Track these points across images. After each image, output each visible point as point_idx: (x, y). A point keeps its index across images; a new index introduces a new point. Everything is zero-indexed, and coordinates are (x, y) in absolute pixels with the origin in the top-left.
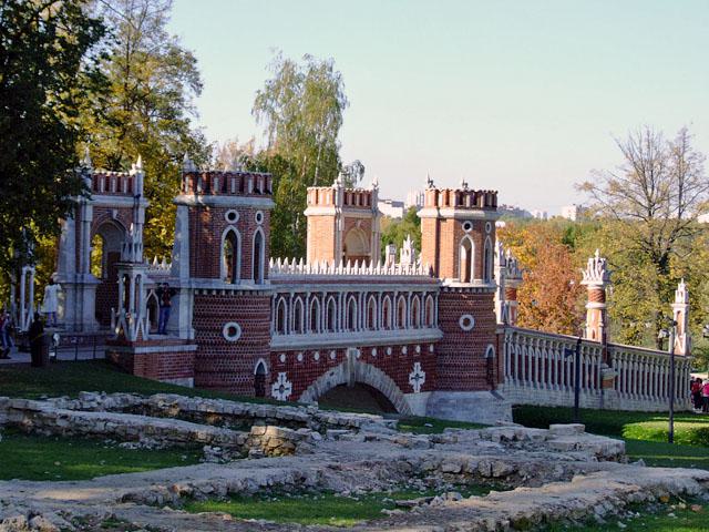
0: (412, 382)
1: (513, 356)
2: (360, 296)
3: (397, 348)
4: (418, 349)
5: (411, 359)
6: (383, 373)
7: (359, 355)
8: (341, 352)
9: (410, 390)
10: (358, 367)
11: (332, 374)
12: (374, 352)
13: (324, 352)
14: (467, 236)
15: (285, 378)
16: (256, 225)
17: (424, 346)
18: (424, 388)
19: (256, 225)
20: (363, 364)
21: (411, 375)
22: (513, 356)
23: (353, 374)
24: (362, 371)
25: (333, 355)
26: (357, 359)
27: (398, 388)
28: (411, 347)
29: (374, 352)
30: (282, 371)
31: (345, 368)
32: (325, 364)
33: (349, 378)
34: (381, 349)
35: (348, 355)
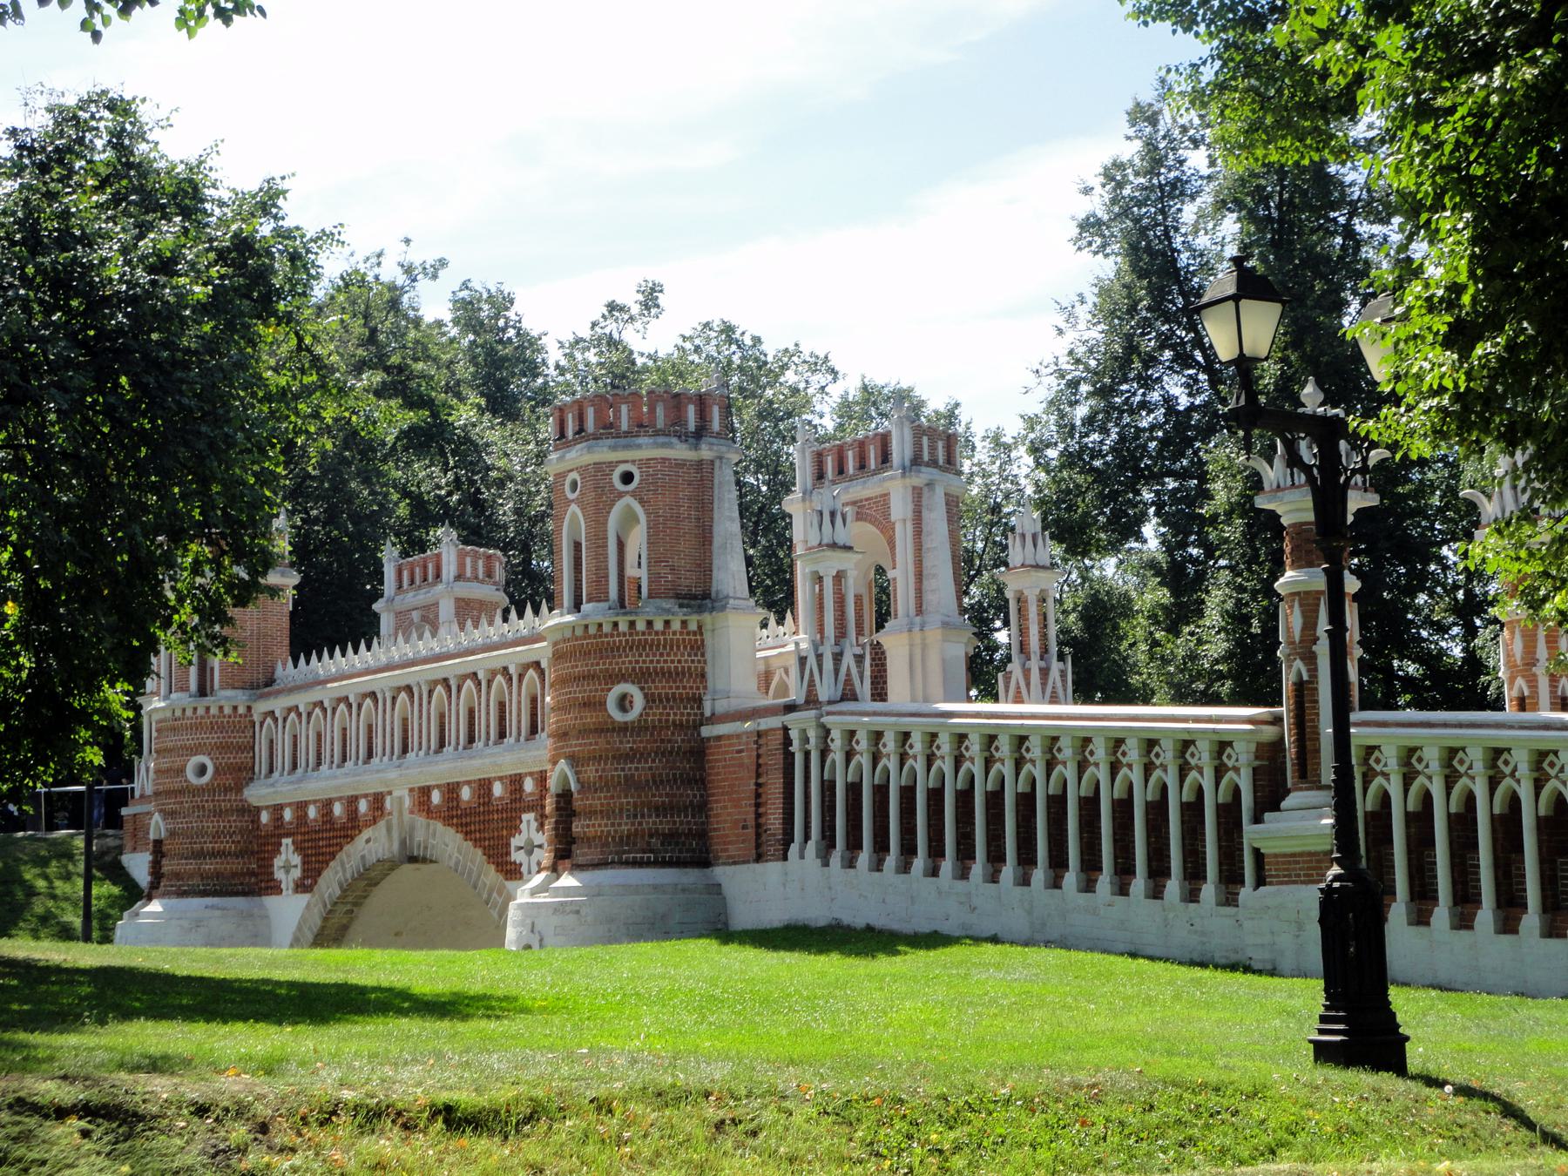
0: (518, 857)
1: (828, 788)
3: (484, 786)
5: (516, 804)
6: (460, 836)
8: (378, 801)
10: (412, 828)
11: (368, 841)
12: (436, 797)
13: (352, 801)
15: (291, 848)
20: (420, 820)
21: (516, 841)
22: (828, 788)
23: (403, 843)
24: (419, 836)
25: (363, 806)
27: (493, 867)
28: (515, 782)
29: (436, 797)
30: (287, 835)
31: (389, 830)
32: (352, 826)
33: (396, 846)
34: (452, 790)
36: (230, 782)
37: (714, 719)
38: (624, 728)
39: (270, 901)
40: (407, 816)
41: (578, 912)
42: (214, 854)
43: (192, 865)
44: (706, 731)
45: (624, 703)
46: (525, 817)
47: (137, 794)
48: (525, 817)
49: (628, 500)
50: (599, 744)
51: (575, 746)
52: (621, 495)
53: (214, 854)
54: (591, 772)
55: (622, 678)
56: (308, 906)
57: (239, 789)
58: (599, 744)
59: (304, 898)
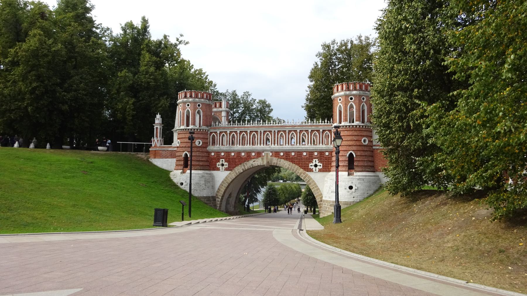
2: (273, 132)
4: (316, 154)
7: (271, 154)
9: (311, 170)
10: (272, 160)
11: (255, 161)
12: (282, 154)
13: (248, 153)
14: (340, 104)
16: (187, 108)
17: (321, 153)
18: (320, 170)
19: (187, 108)
25: (253, 154)
26: (271, 156)
29: (282, 154)
31: (262, 159)
32: (249, 156)
35: (263, 154)
36: (205, 146)
37: (375, 146)
38: (365, 146)
39: (215, 173)
40: (269, 157)
41: (363, 180)
42: (202, 161)
43: (197, 163)
44: (374, 147)
45: (365, 141)
46: (314, 160)
47: (153, 145)
48: (314, 160)
49: (364, 103)
50: (360, 148)
51: (355, 148)
52: (363, 102)
53: (202, 161)
54: (359, 153)
55: (364, 136)
56: (230, 173)
57: (206, 147)
58: (360, 148)
59: (229, 172)
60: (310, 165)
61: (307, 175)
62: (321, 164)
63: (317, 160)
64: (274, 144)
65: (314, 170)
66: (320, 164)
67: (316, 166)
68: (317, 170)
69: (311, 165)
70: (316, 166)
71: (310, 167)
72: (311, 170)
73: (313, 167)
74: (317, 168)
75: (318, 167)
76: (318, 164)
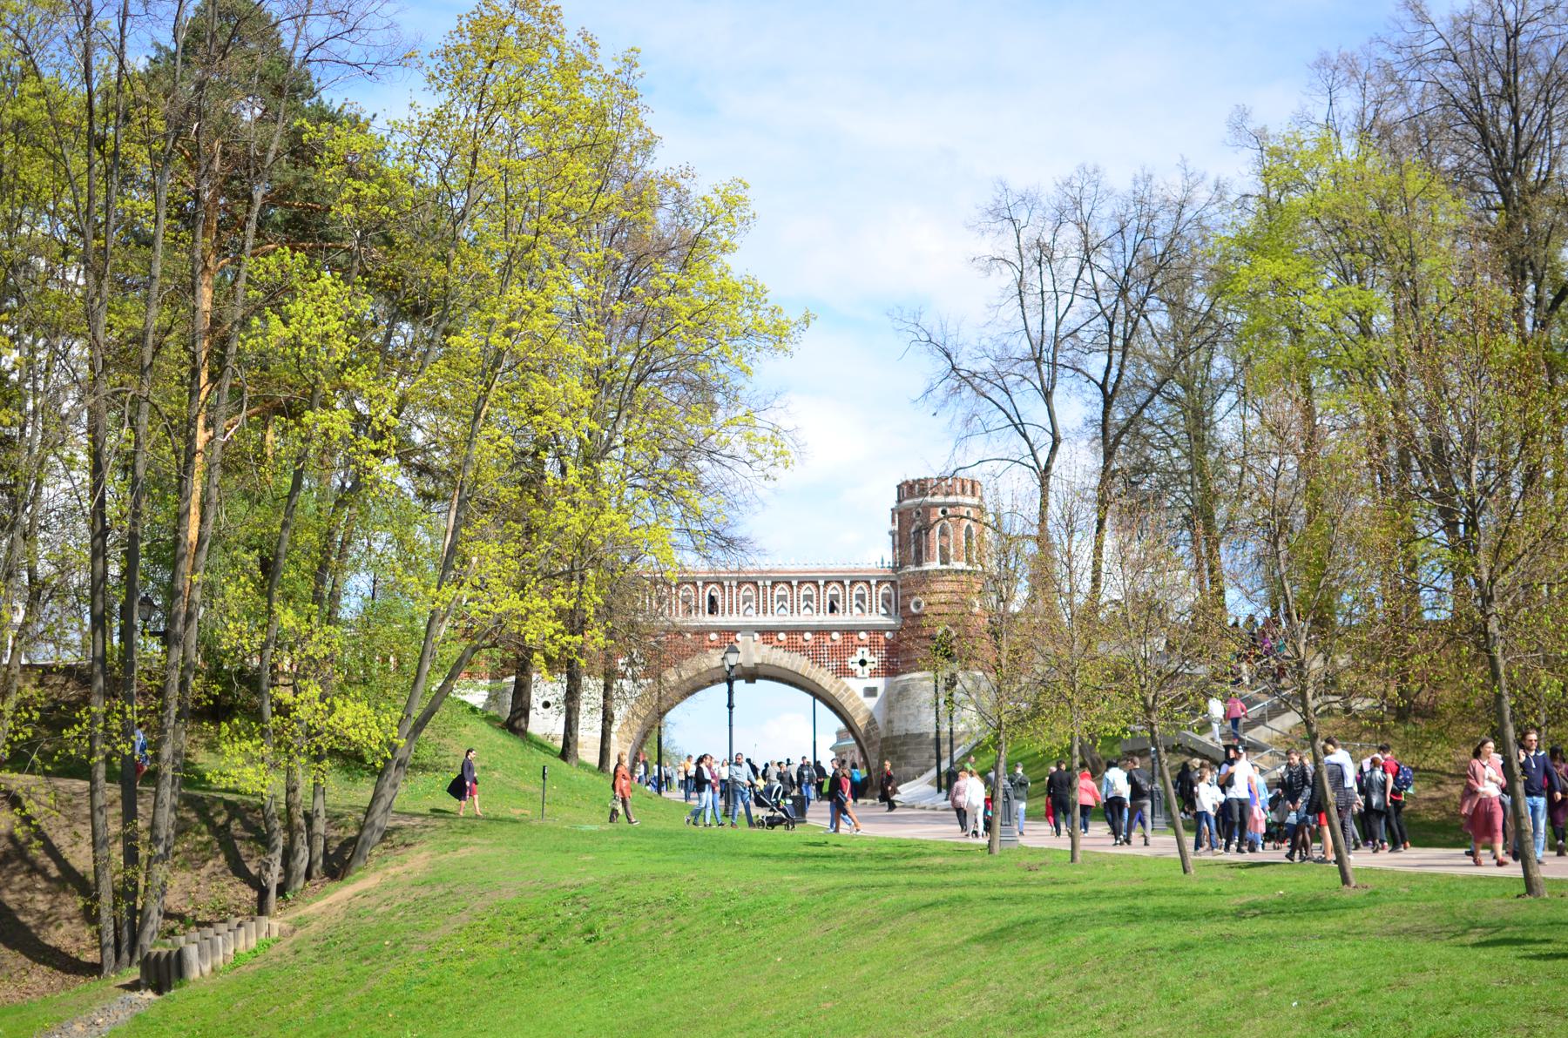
9: (852, 674)
60: (850, 660)
61: (843, 683)
62: (876, 660)
63: (866, 650)
64: (765, 612)
65: (859, 673)
66: (872, 659)
67: (863, 663)
68: (867, 672)
69: (853, 662)
70: (863, 663)
71: (850, 666)
72: (852, 674)
73: (857, 666)
74: (866, 668)
75: (869, 666)
76: (868, 659)
